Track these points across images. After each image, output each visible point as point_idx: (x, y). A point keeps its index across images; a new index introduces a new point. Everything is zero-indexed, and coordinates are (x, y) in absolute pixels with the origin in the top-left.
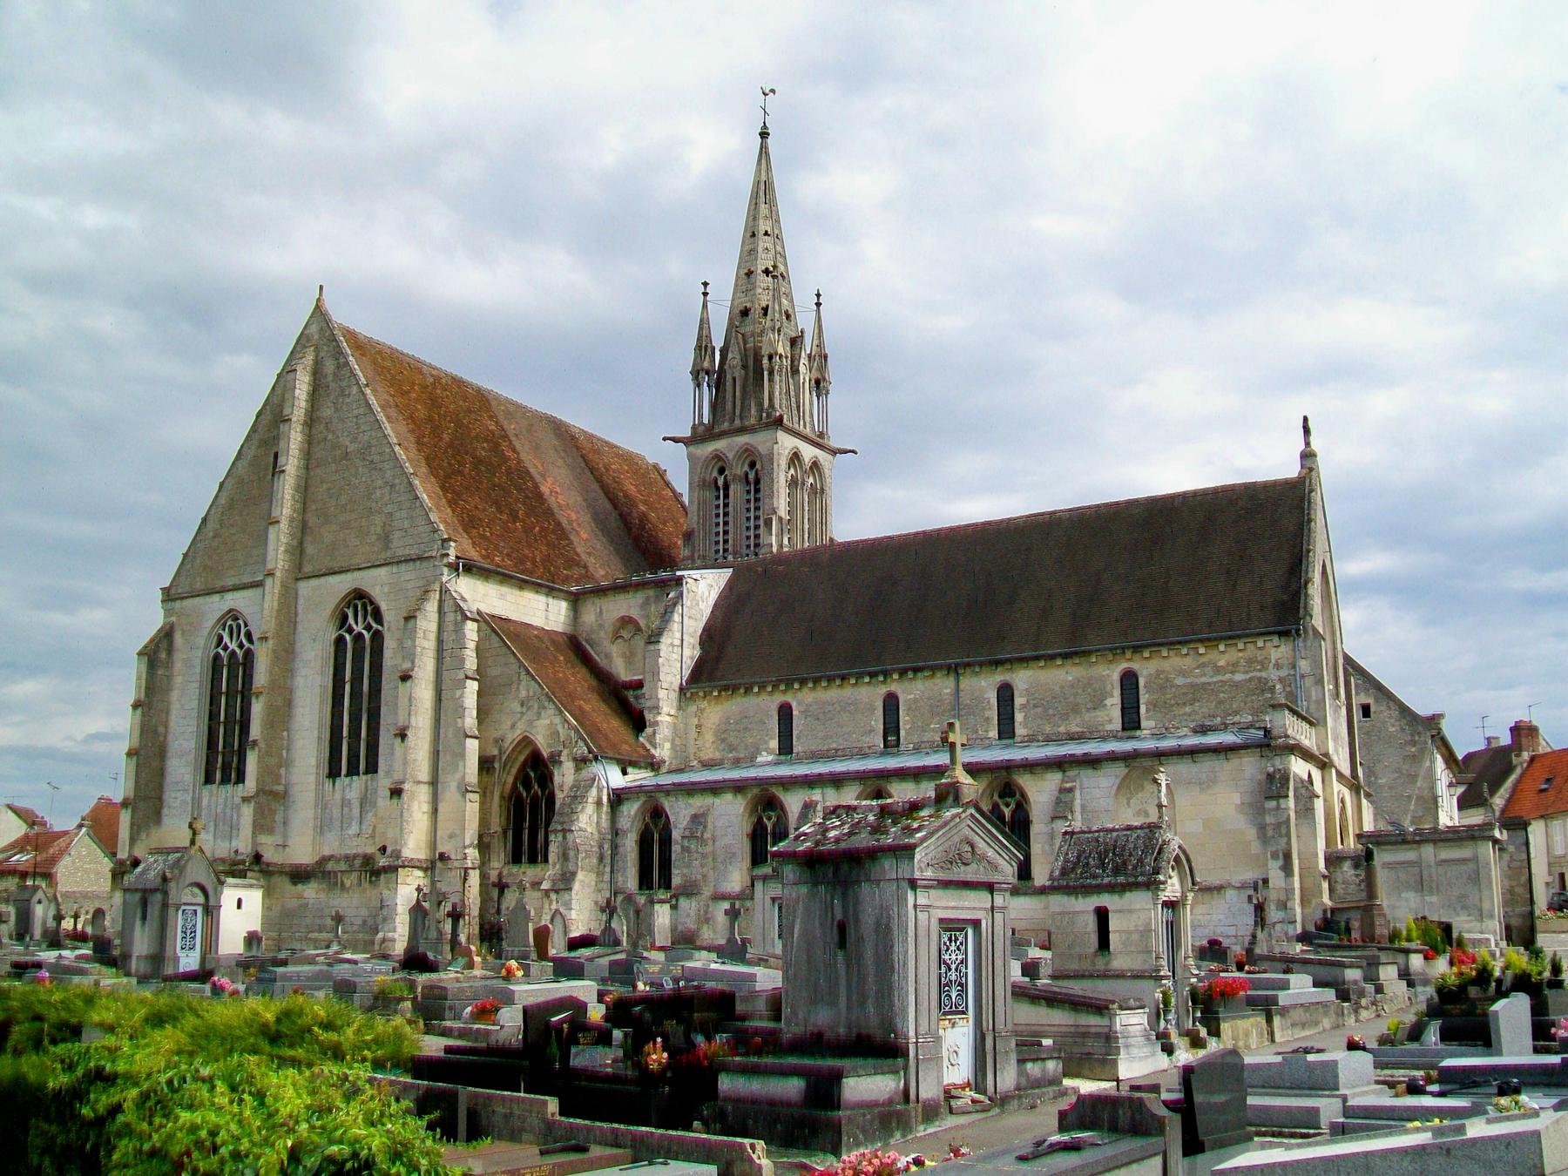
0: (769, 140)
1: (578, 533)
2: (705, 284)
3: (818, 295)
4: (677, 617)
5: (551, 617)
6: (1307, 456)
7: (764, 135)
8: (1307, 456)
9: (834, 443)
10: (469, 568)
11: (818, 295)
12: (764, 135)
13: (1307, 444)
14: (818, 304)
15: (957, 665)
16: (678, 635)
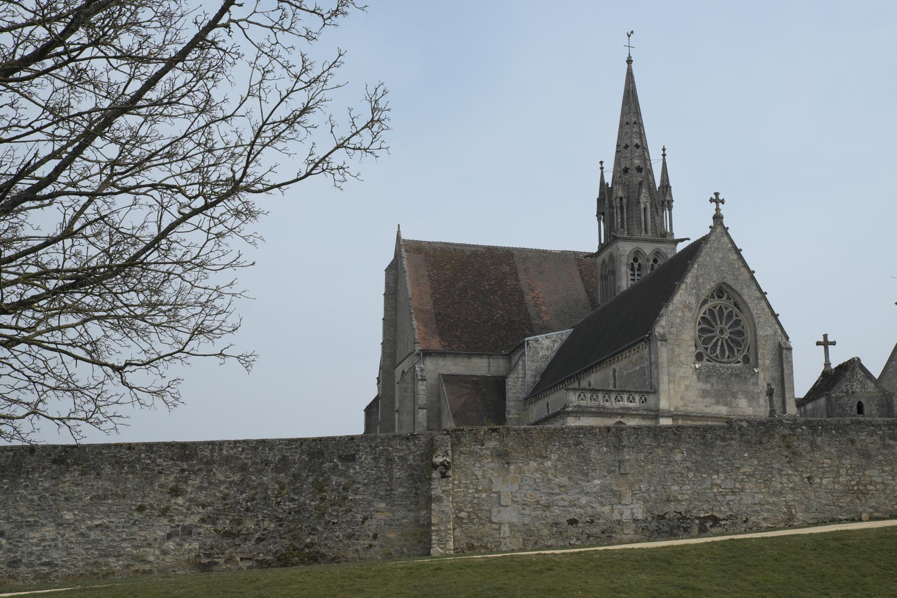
0: (633, 65)
1: (541, 318)
2: (601, 163)
3: (664, 150)
4: (520, 363)
5: (492, 369)
6: (718, 218)
7: (629, 61)
8: (718, 218)
9: (676, 237)
10: (427, 353)
11: (664, 150)
12: (629, 61)
13: (717, 209)
14: (664, 155)
15: (577, 374)
16: (521, 372)
